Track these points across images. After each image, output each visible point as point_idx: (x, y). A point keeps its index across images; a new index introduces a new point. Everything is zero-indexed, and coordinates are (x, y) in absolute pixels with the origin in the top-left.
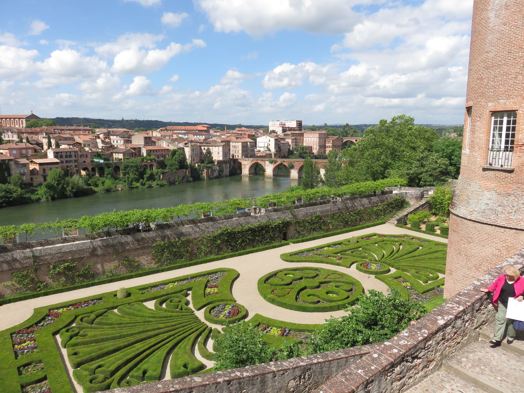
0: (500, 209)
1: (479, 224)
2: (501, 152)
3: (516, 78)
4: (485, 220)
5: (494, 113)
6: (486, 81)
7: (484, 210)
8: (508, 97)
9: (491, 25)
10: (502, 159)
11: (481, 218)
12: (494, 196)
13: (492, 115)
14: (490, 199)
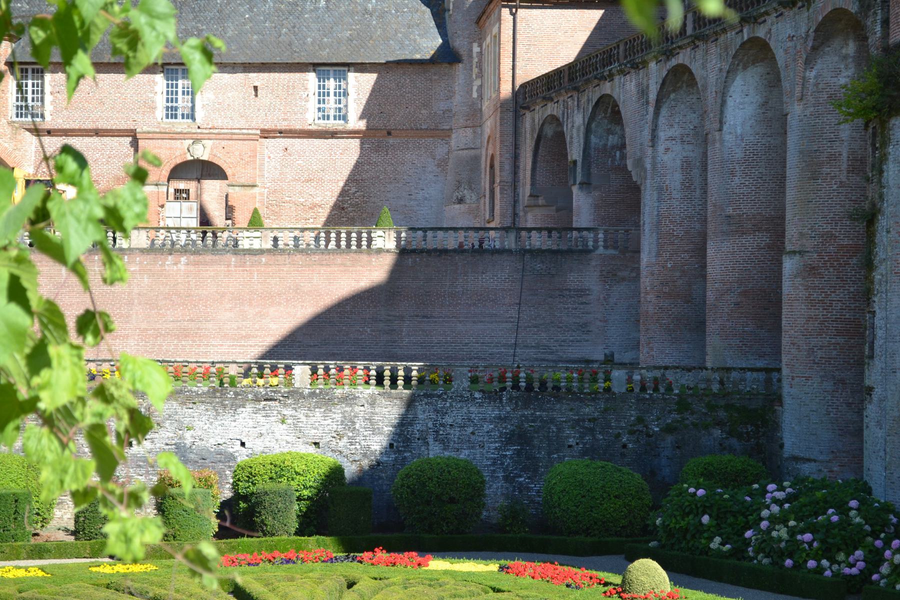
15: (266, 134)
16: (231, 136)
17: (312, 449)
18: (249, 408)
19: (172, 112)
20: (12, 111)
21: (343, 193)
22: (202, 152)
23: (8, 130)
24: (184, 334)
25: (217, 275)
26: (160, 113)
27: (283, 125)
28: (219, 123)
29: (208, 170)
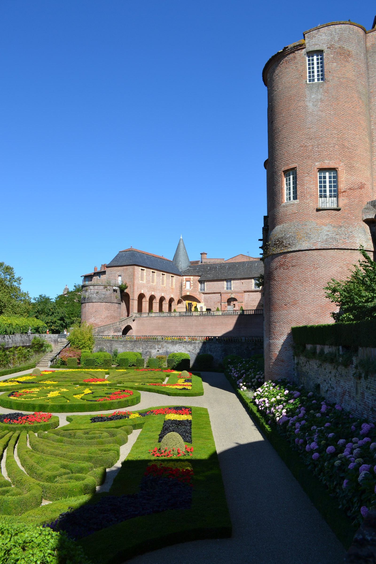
0: (337, 237)
1: (324, 251)
2: (328, 198)
3: (334, 147)
4: (329, 246)
5: (321, 170)
6: (310, 148)
7: (326, 239)
8: (331, 159)
9: (310, 110)
10: (330, 202)
11: (326, 246)
12: (331, 229)
13: (319, 171)
14: (328, 231)
15: (245, 292)
16: (238, 293)
17: (188, 352)
18: (178, 345)
19: (227, 288)
20: (199, 290)
21: (259, 303)
22: (233, 296)
23: (199, 293)
24: (202, 332)
25: (209, 320)
26: (225, 289)
27: (248, 290)
28: (236, 290)
29: (235, 300)
